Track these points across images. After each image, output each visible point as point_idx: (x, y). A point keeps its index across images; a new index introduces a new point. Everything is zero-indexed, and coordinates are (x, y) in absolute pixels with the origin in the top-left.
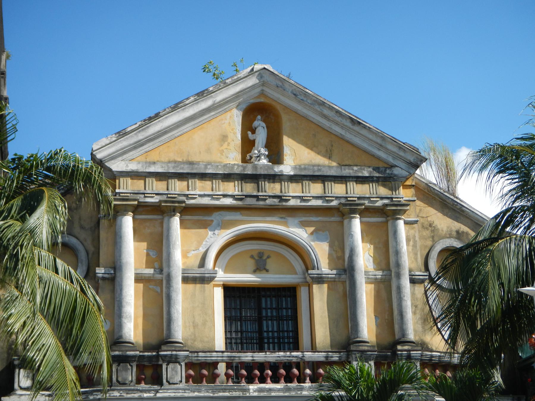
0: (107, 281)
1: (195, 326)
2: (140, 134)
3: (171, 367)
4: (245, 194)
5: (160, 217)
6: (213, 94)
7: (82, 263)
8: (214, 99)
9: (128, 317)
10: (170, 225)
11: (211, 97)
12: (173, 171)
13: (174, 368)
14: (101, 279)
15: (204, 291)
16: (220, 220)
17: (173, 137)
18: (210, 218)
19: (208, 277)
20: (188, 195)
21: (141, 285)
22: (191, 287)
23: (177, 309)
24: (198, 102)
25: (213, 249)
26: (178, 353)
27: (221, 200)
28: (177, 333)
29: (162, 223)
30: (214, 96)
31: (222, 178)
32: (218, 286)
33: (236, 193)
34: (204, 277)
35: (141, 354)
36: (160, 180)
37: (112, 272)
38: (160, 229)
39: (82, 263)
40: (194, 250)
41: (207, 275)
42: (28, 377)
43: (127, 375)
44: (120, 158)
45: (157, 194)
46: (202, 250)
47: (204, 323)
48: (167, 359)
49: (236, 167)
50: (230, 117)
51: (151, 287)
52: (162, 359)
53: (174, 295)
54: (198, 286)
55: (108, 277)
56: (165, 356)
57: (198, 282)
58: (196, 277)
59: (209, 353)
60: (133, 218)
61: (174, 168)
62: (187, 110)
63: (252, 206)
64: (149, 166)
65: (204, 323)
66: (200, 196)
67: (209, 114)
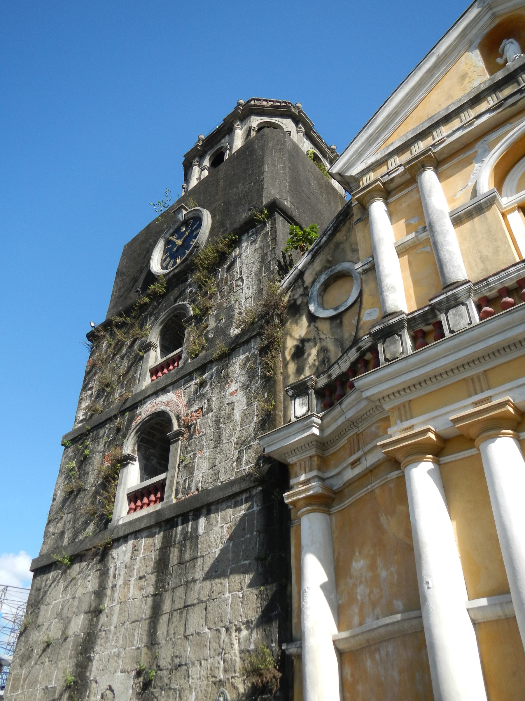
0: (369, 272)
1: (483, 259)
2: (369, 130)
3: (451, 314)
4: (503, 99)
5: (414, 186)
6: (433, 51)
7: (356, 279)
8: (438, 54)
9: (390, 288)
10: (422, 181)
11: (433, 54)
12: (412, 136)
13: (457, 312)
14: (363, 274)
15: (486, 219)
16: (485, 146)
17: (407, 114)
18: (472, 152)
19: (485, 202)
20: (435, 144)
21: (406, 257)
22: (467, 226)
23: (448, 250)
24: (420, 67)
25: (483, 174)
26: (455, 291)
27: (475, 123)
28: (453, 274)
29: (418, 191)
30: (435, 52)
31: (470, 106)
32: (512, 211)
33: (492, 103)
34: (480, 204)
35: (410, 317)
36: (403, 154)
37: (371, 259)
38: (418, 196)
39: (356, 279)
40: (461, 190)
41: (482, 201)
42: (303, 404)
43: (396, 347)
44: (359, 162)
45: (400, 166)
46: (471, 184)
47: (496, 251)
48: (444, 306)
49: (482, 85)
50: (466, 58)
51: (418, 252)
52: (439, 311)
53: (440, 239)
54: (477, 220)
55: (368, 267)
56: (440, 302)
57: (474, 215)
58: (469, 210)
59: (503, 273)
60: (387, 204)
61: (412, 134)
62: (411, 81)
63: (519, 103)
64: (388, 149)
65: (496, 251)
66: (449, 136)
67: (440, 71)
